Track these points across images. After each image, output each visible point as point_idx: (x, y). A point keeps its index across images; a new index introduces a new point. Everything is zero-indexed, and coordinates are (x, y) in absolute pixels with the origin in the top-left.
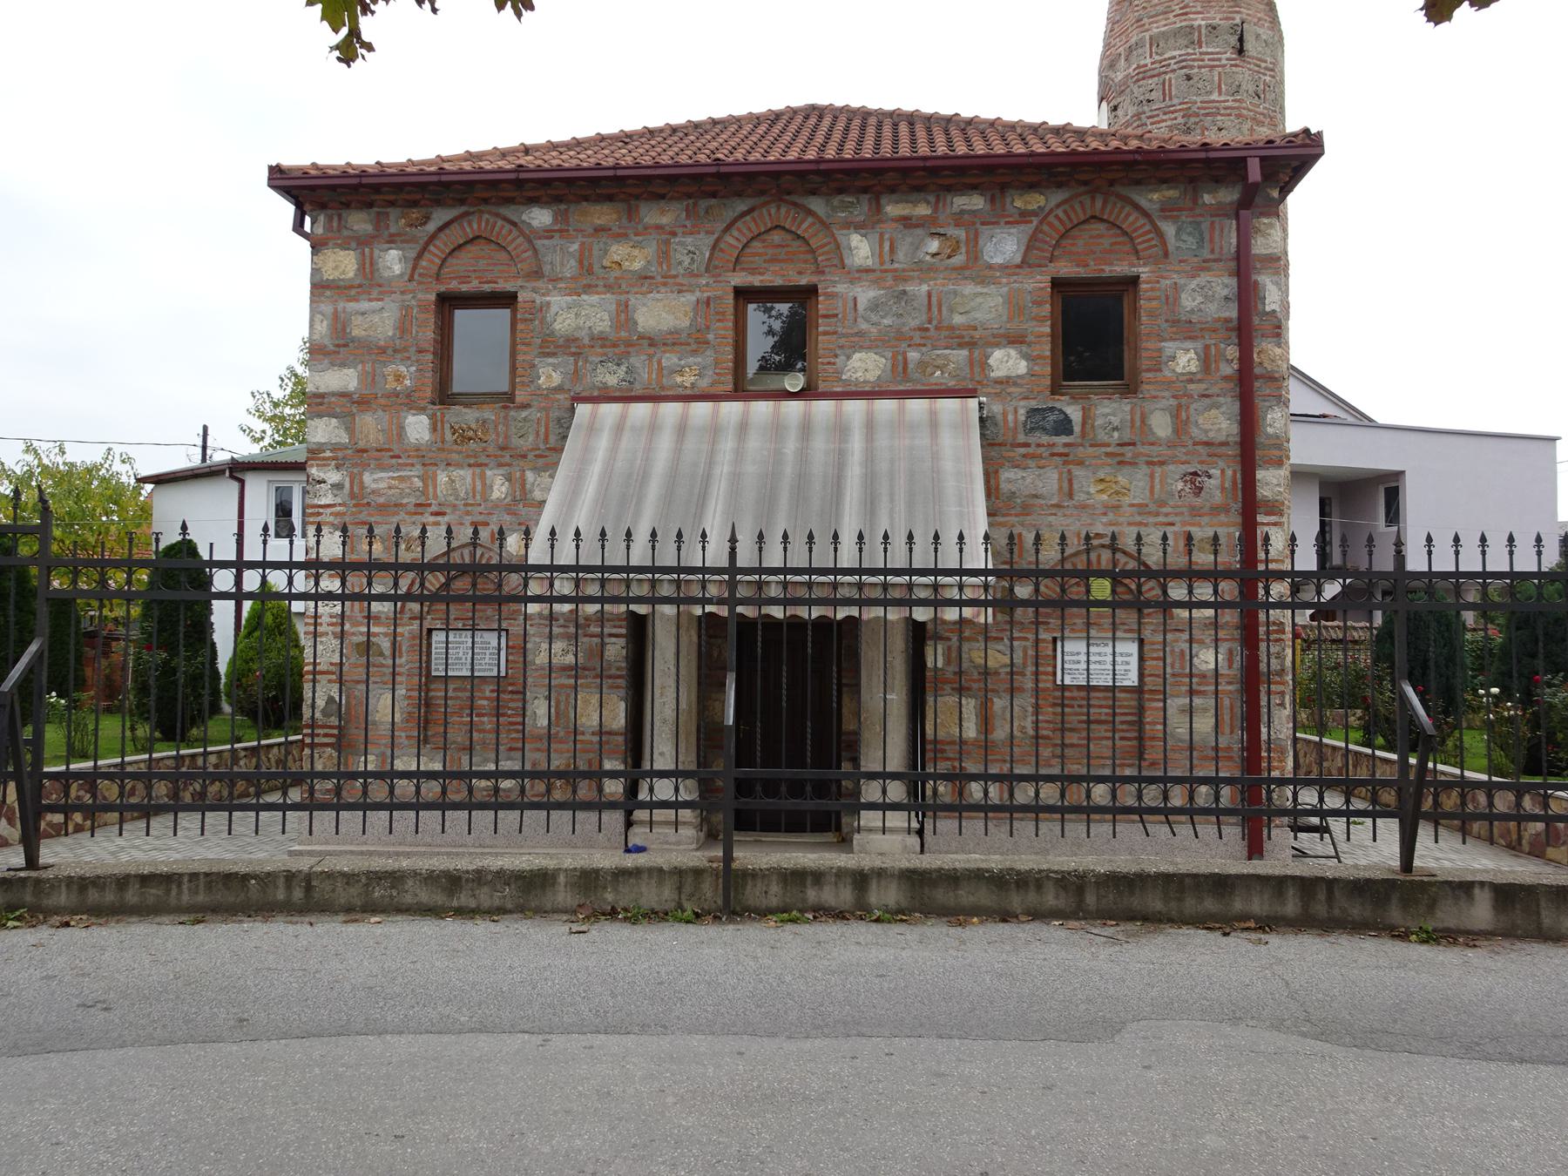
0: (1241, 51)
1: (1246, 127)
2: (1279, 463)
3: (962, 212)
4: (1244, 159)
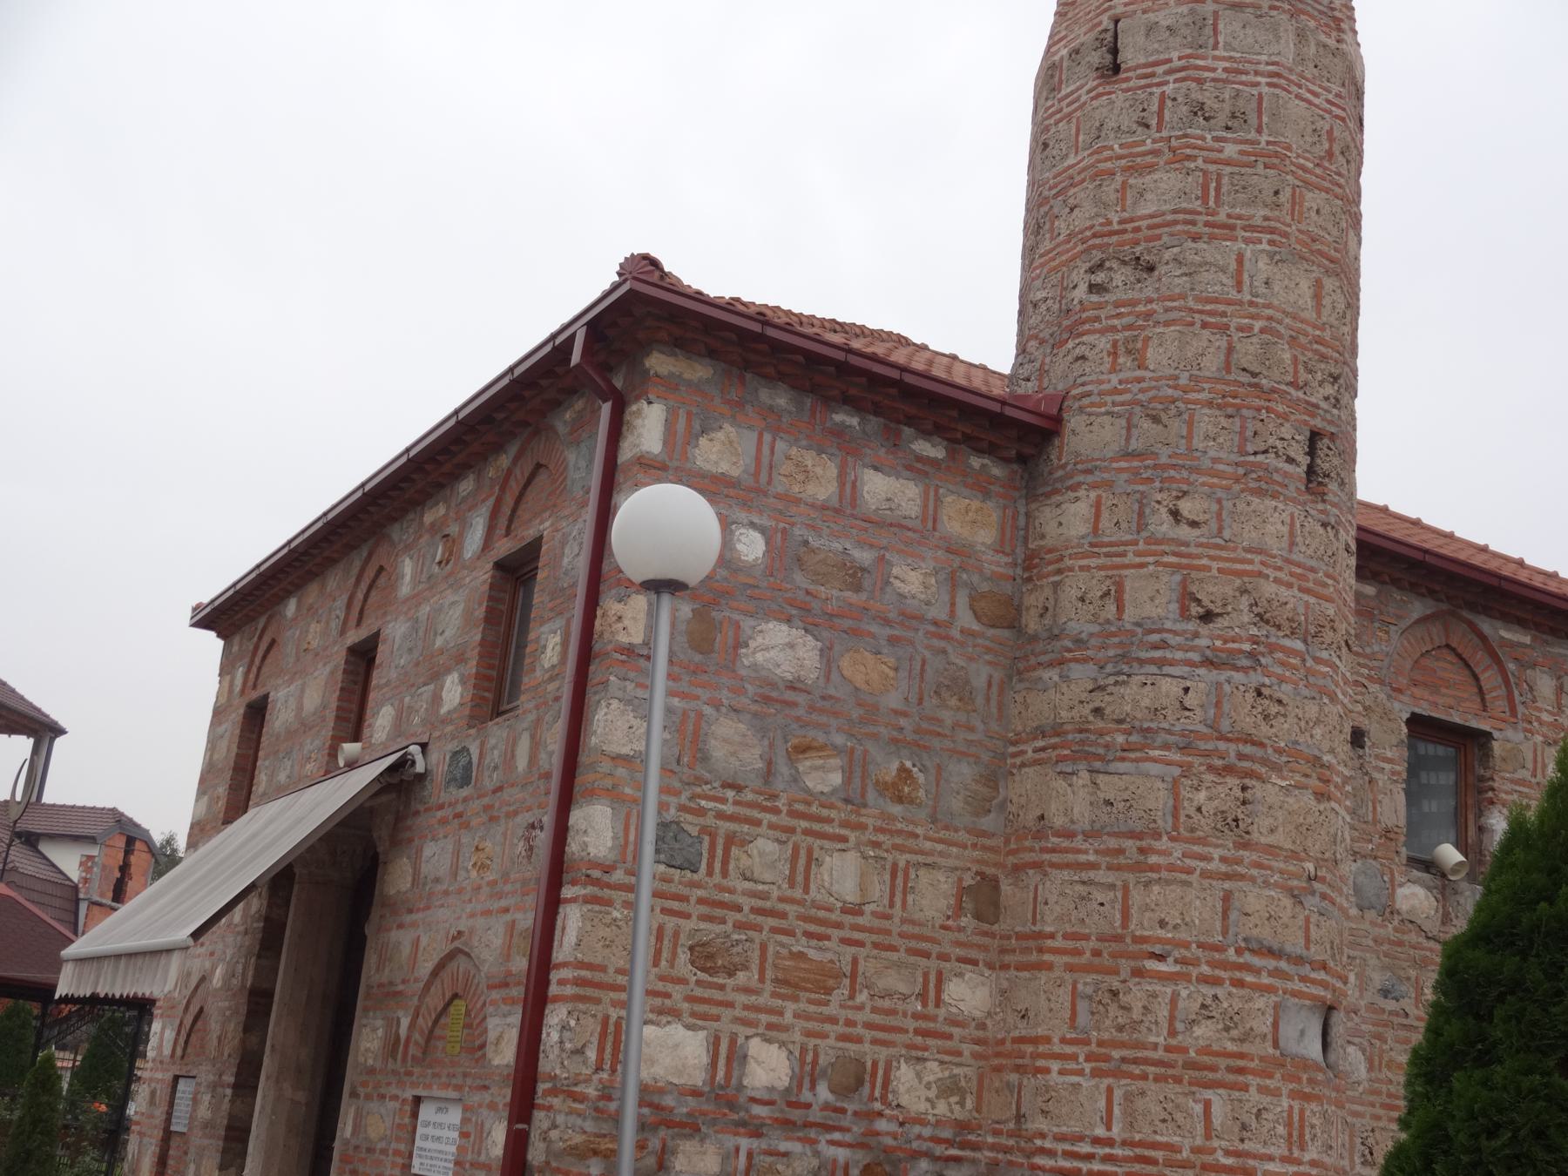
0: (1116, 68)
1: (1110, 191)
2: (591, 794)
3: (464, 499)
4: (572, 337)
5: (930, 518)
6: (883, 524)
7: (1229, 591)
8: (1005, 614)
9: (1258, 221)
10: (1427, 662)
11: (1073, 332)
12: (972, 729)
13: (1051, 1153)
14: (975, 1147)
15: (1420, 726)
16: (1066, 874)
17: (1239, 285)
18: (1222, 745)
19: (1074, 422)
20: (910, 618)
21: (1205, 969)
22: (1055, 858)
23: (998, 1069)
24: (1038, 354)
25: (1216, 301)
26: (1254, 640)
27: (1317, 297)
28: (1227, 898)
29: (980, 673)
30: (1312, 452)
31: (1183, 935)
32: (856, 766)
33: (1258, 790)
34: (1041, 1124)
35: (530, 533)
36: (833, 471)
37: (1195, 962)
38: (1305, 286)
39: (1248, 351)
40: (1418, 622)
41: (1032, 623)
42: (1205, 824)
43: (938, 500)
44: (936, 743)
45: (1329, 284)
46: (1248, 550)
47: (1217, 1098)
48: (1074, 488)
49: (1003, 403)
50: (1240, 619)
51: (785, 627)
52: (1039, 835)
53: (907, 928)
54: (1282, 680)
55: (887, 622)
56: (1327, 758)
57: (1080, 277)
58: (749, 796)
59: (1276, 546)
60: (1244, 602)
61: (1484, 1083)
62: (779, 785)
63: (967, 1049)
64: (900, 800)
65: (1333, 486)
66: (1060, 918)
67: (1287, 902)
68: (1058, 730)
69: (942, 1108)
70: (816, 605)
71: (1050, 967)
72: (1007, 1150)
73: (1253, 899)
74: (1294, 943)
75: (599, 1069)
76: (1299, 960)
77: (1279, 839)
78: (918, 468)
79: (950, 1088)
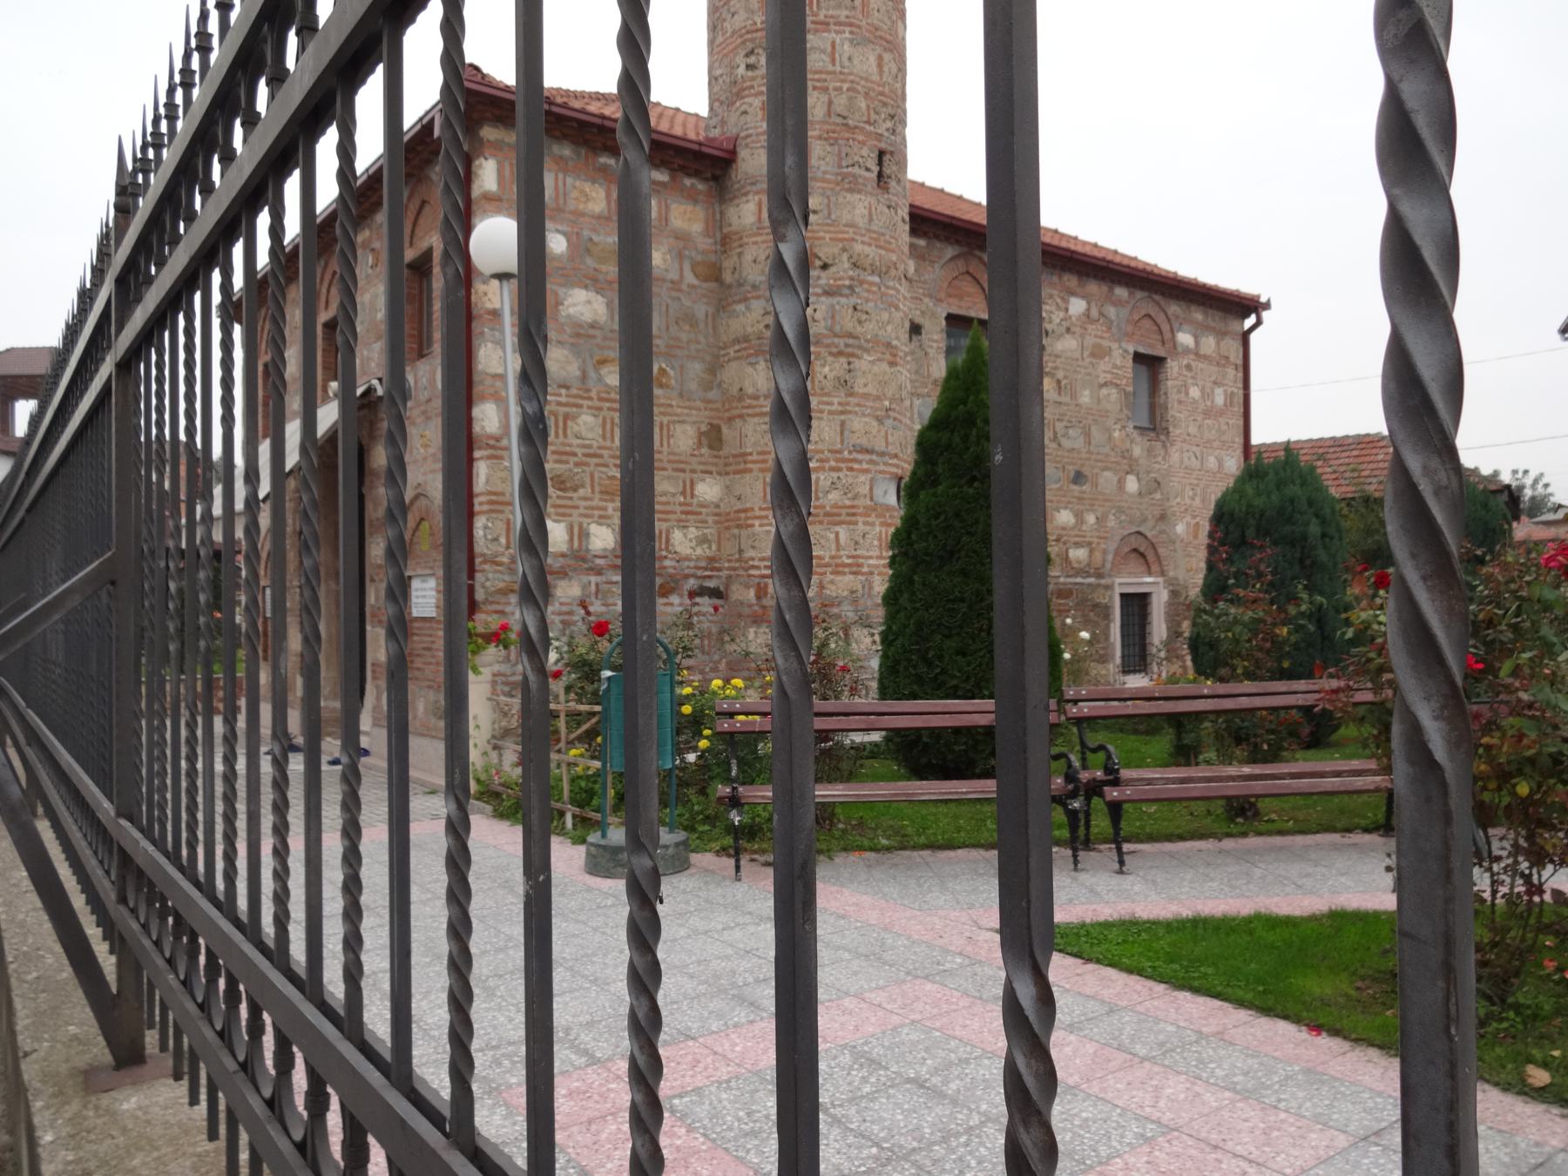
2: (483, 398)
4: (432, 120)
7: (836, 250)
8: (713, 273)
9: (843, 19)
10: (956, 282)
11: (739, 95)
12: (698, 343)
13: (758, 568)
14: (719, 570)
15: (952, 319)
16: (756, 420)
17: (833, 61)
18: (836, 340)
19: (743, 153)
21: (833, 463)
22: (750, 411)
23: (728, 528)
24: (720, 111)
25: (820, 72)
26: (852, 279)
27: (880, 66)
28: (843, 424)
29: (701, 310)
30: (880, 163)
31: (820, 446)
33: (857, 363)
34: (751, 553)
35: (424, 245)
36: (602, 194)
37: (827, 460)
38: (872, 59)
39: (841, 102)
40: (952, 259)
41: (728, 277)
42: (829, 385)
44: (679, 352)
45: (887, 56)
46: (846, 225)
47: (843, 531)
48: (745, 194)
49: (700, 144)
50: (843, 267)
51: (584, 292)
52: (740, 399)
53: (672, 457)
54: (867, 300)
56: (895, 342)
57: (741, 61)
58: (574, 391)
59: (862, 223)
60: (845, 257)
61: (935, 495)
62: (590, 383)
63: (710, 519)
65: (893, 184)
66: (755, 444)
67: (875, 423)
68: (746, 339)
69: (699, 551)
70: (601, 277)
71: (751, 471)
72: (735, 569)
73: (857, 423)
74: (880, 445)
75: (508, 547)
76: (882, 454)
77: (870, 389)
79: (703, 540)
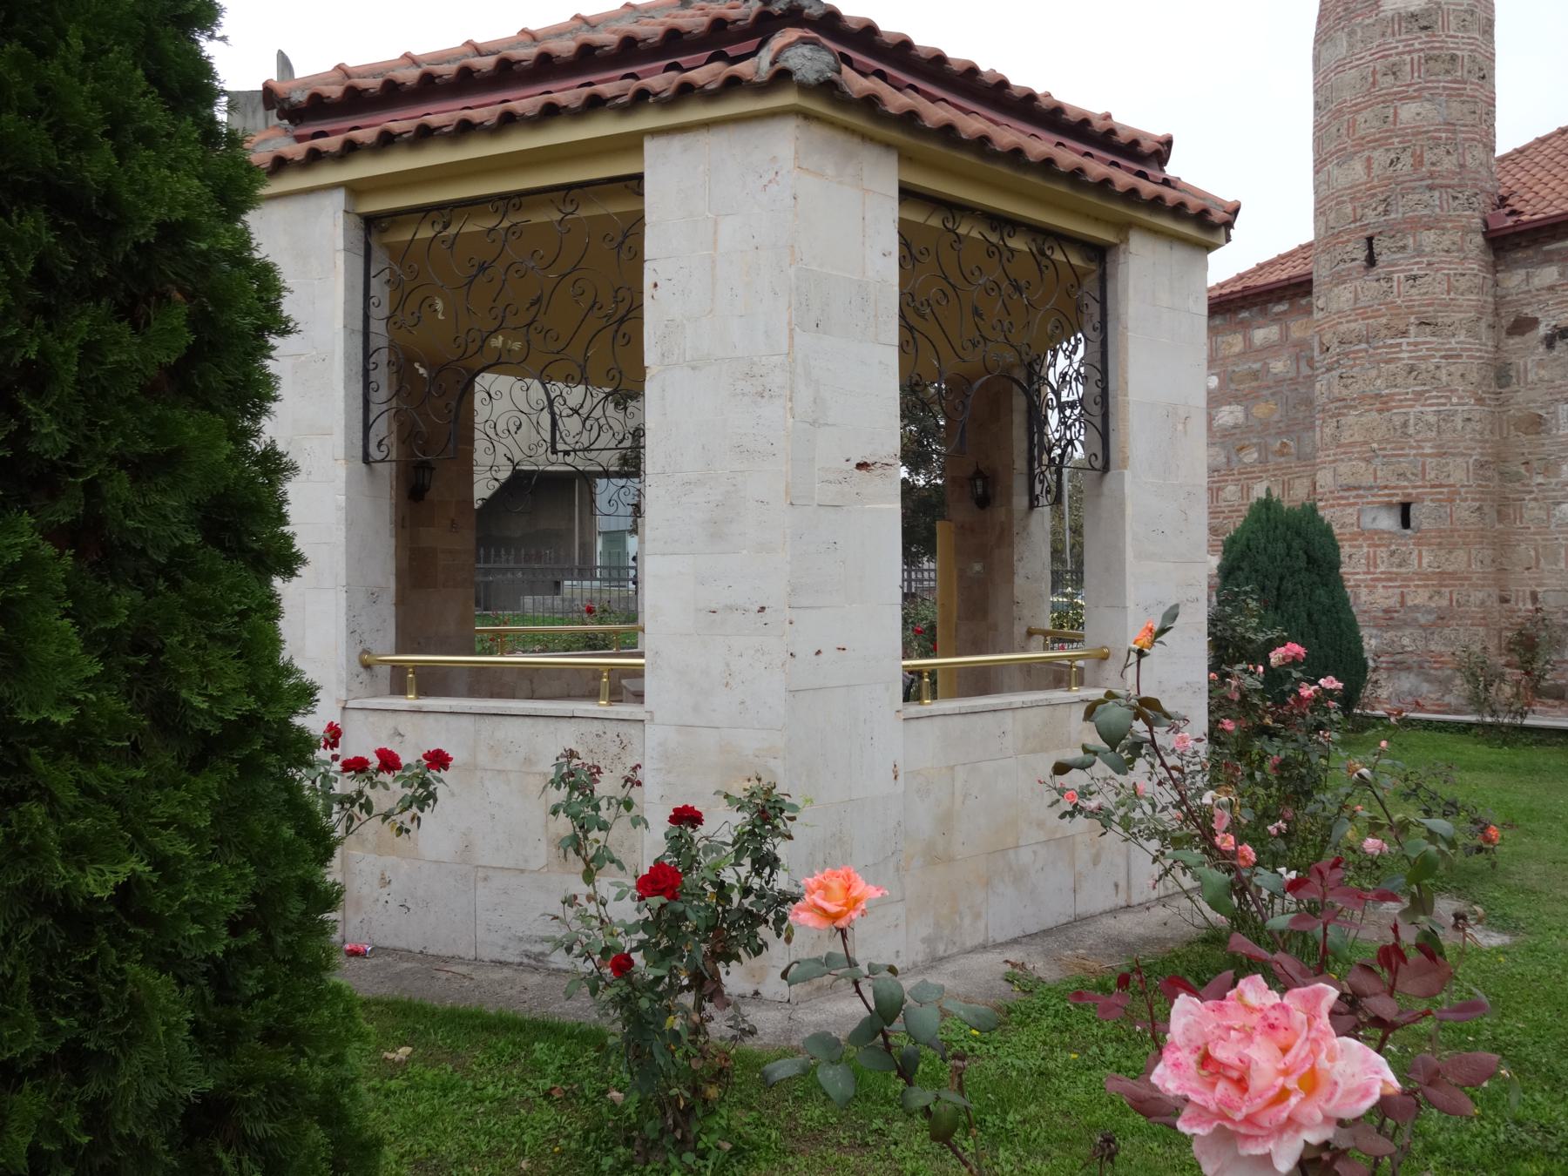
5: (1285, 335)
6: (1270, 349)
20: (1279, 381)
32: (1263, 448)
33: (1343, 420)
36: (1240, 337)
38: (1358, 166)
43: (1288, 328)
55: (1269, 388)
64: (1283, 455)
67: (1363, 464)
76: (1371, 488)
77: (1357, 438)
78: (1277, 319)
